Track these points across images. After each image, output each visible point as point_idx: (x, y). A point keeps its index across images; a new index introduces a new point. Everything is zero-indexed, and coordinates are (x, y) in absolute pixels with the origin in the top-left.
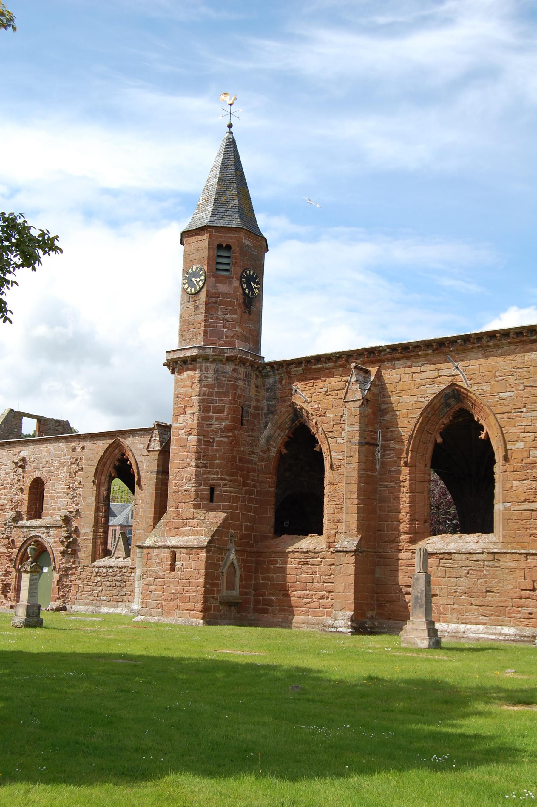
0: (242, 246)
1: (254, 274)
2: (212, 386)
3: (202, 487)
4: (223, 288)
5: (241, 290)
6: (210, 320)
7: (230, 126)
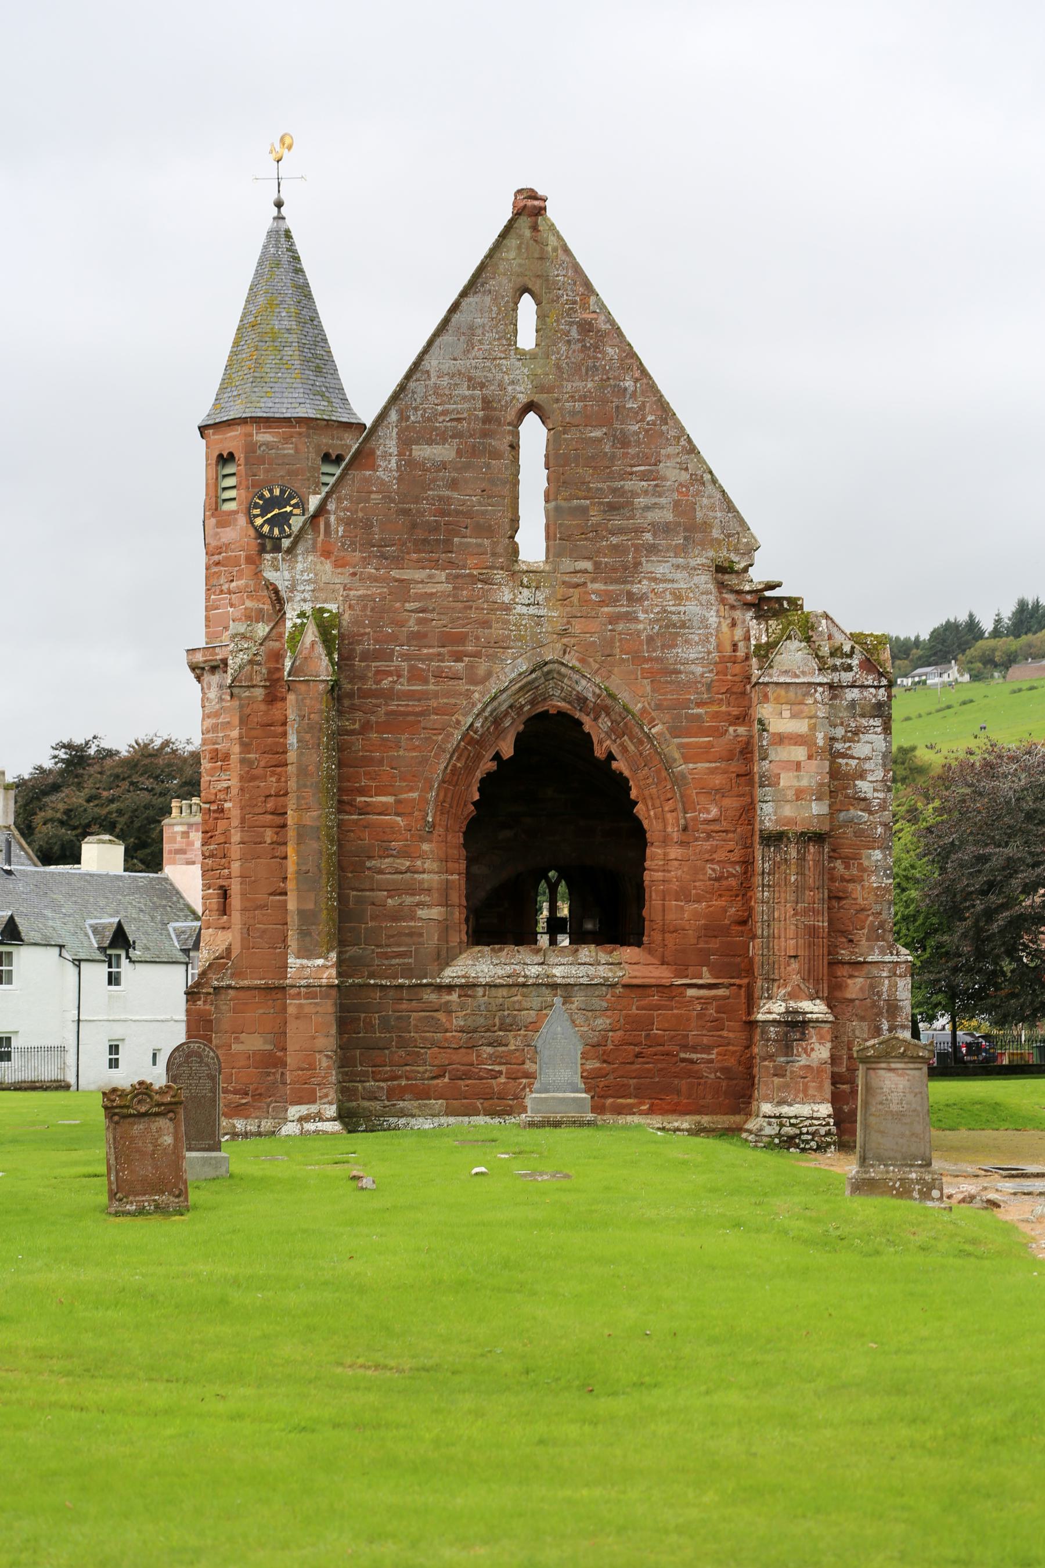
0: (251, 448)
1: (282, 492)
2: (216, 714)
3: (211, 891)
4: (229, 535)
5: (252, 532)
6: (213, 597)
7: (279, 204)
